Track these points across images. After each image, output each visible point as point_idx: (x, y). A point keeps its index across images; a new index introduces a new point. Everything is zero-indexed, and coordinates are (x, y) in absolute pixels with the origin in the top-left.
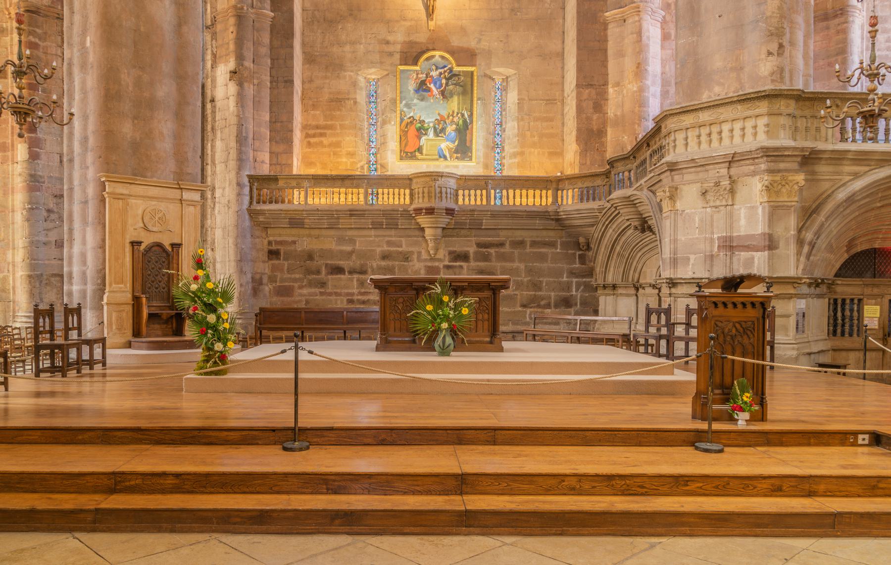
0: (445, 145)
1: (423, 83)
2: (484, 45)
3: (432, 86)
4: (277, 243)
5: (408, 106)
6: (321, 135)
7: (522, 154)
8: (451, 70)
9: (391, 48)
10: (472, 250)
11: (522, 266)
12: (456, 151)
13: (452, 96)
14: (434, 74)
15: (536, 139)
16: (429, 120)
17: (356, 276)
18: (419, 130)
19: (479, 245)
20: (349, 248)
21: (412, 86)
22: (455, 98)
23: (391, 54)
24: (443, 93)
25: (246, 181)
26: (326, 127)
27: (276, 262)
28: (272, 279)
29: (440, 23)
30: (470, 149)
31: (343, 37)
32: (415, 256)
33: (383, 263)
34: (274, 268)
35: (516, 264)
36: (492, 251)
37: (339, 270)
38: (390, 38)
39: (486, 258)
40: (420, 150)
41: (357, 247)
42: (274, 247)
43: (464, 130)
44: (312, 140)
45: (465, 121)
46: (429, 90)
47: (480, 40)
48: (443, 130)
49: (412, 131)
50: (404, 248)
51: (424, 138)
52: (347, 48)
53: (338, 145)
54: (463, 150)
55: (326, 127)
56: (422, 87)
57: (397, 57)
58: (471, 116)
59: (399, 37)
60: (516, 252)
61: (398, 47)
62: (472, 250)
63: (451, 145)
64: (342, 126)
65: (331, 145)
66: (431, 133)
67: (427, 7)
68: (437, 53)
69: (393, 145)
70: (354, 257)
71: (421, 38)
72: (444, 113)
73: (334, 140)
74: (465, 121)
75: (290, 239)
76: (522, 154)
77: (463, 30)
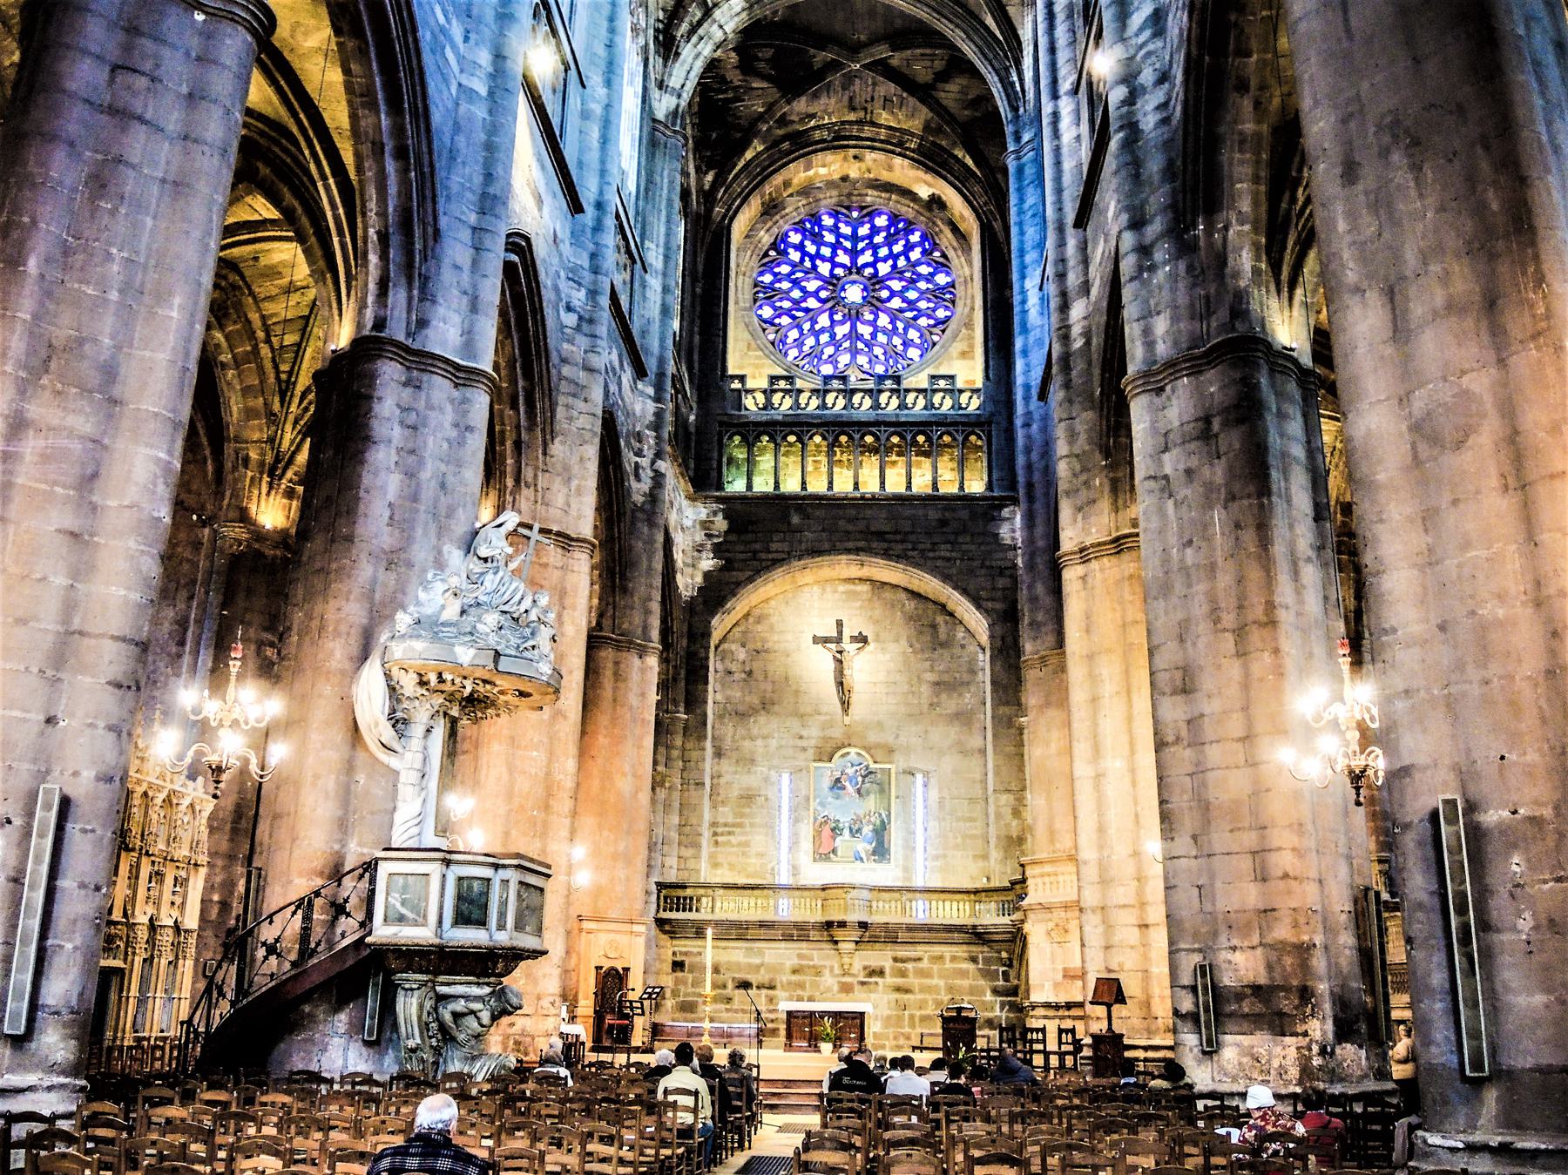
0: (864, 847)
1: (838, 780)
2: (903, 740)
3: (847, 784)
4: (686, 954)
5: (822, 804)
6: (729, 833)
7: (945, 856)
8: (867, 767)
9: (804, 743)
10: (888, 965)
11: (942, 983)
12: (874, 853)
13: (868, 793)
14: (850, 771)
15: (959, 840)
16: (845, 820)
17: (764, 992)
18: (833, 830)
19: (895, 960)
20: (757, 961)
21: (827, 783)
22: (872, 796)
23: (804, 749)
24: (859, 791)
25: (654, 888)
26: (734, 825)
27: (680, 974)
28: (675, 993)
29: (857, 718)
30: (888, 851)
31: (755, 731)
32: (827, 972)
33: (794, 978)
34: (677, 981)
35: (935, 981)
36: (910, 966)
37: (745, 985)
38: (804, 733)
39: (903, 974)
40: (834, 851)
41: (767, 960)
42: (679, 958)
43: (881, 832)
44: (720, 839)
45: (883, 822)
46: (844, 788)
47: (897, 736)
48: (859, 830)
49: (827, 830)
50: (816, 962)
51: (839, 839)
52: (759, 742)
53: (746, 844)
54: (880, 851)
55: (734, 825)
56: (837, 784)
57: (811, 753)
58: (889, 816)
59: (813, 733)
60: (935, 967)
61: (813, 742)
62: (888, 965)
63: (870, 848)
64: (752, 825)
65: (739, 844)
66: (846, 832)
67: (843, 703)
68: (853, 750)
69: (806, 845)
70: (762, 971)
71: (837, 733)
72: (861, 813)
73: (743, 839)
74: (883, 822)
75: (695, 950)
76: (945, 856)
77: (880, 725)
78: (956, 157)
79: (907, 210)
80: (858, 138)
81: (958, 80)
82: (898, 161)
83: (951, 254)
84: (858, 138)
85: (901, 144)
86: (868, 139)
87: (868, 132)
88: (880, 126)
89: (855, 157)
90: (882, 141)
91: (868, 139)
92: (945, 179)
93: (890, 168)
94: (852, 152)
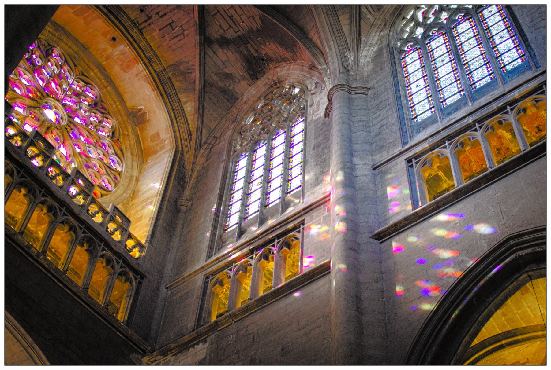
78: (179, 101)
79: (111, 103)
80: (126, 29)
81: (229, 53)
82: (141, 67)
83: (128, 154)
84: (126, 29)
85: (149, 60)
86: (132, 37)
87: (135, 32)
88: (144, 38)
89: (114, 39)
90: (140, 47)
91: (132, 37)
92: (166, 104)
93: (126, 68)
94: (117, 34)
